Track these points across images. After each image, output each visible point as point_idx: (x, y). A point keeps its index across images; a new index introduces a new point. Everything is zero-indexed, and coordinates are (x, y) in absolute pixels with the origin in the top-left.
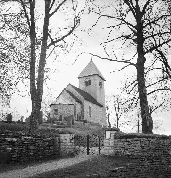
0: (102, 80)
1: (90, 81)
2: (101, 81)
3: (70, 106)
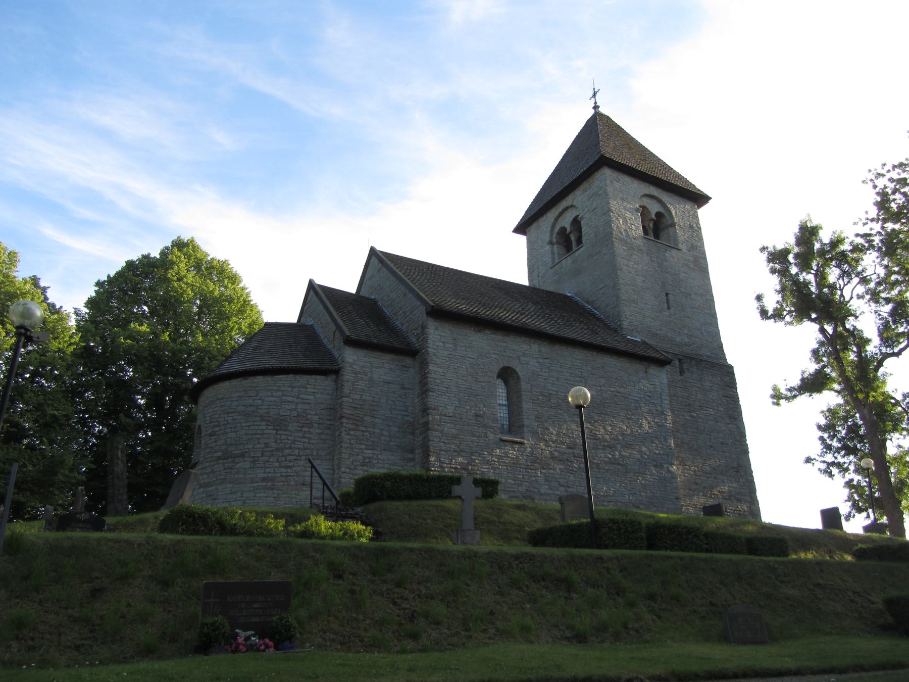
0: (666, 197)
1: (576, 222)
2: (660, 201)
3: (284, 380)
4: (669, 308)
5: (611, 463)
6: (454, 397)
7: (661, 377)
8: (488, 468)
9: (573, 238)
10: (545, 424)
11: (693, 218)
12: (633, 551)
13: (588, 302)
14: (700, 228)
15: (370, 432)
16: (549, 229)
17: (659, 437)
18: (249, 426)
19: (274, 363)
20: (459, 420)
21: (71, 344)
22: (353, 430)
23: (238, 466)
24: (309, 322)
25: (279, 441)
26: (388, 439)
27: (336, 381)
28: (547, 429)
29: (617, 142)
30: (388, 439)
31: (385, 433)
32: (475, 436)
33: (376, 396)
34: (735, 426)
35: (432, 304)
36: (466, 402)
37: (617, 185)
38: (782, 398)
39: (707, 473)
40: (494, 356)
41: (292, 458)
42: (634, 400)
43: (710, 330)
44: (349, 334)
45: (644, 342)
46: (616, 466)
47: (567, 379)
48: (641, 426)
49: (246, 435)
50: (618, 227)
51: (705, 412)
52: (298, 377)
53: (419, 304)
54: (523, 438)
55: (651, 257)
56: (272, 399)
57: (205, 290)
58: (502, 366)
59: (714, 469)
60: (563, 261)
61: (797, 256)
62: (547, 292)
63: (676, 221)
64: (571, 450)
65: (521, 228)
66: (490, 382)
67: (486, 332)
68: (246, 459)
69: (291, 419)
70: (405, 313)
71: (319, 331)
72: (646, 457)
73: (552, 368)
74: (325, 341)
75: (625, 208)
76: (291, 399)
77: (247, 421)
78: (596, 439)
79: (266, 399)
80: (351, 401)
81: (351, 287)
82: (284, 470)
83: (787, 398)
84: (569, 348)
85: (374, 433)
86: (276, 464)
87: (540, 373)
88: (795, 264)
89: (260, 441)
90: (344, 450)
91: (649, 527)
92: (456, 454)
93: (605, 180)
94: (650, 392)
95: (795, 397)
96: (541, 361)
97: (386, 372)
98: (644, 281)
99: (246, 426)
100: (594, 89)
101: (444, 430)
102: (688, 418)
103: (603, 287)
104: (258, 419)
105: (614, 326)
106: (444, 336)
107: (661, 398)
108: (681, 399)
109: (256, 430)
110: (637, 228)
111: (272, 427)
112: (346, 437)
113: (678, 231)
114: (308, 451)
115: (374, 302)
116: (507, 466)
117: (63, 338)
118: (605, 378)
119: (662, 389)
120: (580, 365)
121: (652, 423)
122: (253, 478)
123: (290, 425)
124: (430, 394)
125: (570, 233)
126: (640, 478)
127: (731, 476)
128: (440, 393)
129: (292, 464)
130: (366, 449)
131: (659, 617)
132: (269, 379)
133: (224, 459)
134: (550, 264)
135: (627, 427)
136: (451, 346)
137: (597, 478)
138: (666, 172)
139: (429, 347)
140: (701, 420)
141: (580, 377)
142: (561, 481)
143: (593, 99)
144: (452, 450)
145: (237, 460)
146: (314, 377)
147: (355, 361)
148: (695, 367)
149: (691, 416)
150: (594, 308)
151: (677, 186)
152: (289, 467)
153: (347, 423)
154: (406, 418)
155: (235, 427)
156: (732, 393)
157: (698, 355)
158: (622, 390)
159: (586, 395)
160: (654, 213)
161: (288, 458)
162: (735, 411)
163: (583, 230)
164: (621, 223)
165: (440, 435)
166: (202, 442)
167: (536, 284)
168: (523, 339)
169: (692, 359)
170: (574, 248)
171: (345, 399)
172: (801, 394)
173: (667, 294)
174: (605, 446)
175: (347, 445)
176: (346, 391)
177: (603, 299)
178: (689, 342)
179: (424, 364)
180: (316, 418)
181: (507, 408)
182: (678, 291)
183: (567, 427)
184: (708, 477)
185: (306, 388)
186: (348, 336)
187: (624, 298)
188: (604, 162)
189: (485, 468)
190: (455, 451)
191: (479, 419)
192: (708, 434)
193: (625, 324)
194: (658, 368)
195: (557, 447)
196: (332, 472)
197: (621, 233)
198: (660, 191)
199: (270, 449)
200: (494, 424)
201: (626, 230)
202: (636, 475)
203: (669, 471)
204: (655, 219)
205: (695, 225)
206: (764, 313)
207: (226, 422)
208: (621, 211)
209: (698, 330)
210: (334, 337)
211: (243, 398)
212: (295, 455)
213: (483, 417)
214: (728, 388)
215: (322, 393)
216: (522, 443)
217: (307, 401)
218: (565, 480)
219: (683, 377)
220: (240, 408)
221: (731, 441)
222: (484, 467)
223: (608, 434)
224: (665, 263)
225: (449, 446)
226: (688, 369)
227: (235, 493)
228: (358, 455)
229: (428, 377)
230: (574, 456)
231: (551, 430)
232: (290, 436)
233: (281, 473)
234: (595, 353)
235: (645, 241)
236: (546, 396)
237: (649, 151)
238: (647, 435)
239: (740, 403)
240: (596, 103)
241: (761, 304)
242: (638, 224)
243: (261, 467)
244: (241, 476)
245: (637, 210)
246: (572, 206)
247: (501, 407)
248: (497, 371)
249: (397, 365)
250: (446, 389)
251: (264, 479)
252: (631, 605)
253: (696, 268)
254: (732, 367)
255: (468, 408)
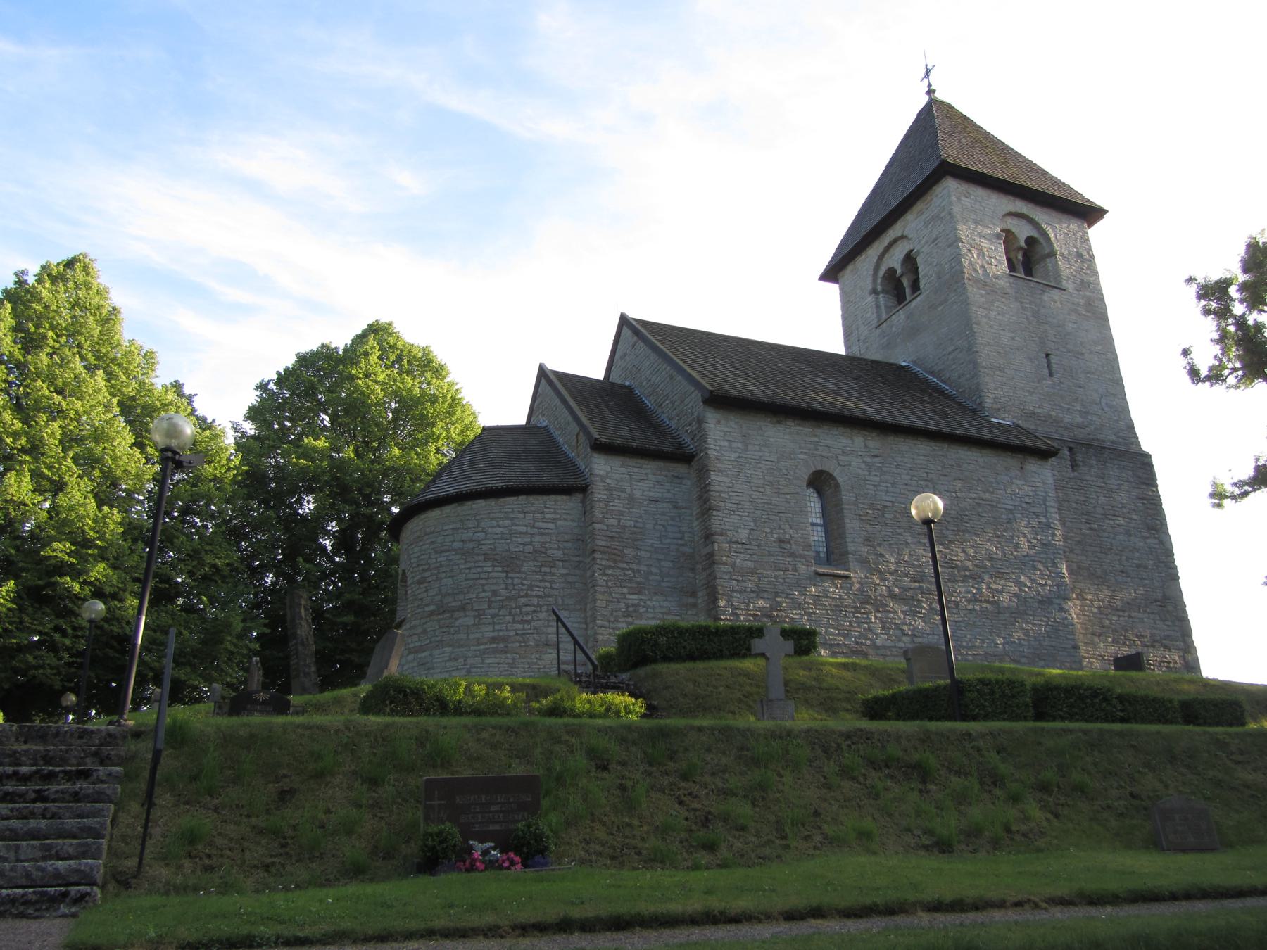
0: (1039, 215)
1: (910, 260)
3: (512, 504)
4: (1051, 375)
5: (977, 600)
6: (748, 516)
7: (1044, 475)
8: (800, 614)
9: (906, 282)
10: (878, 548)
11: (1082, 243)
12: (1014, 724)
13: (932, 373)
14: (1092, 256)
15: (633, 570)
16: (871, 272)
17: (1044, 561)
18: (469, 568)
19: (497, 482)
20: (756, 548)
21: (229, 469)
22: (610, 567)
23: (457, 623)
24: (543, 422)
25: (511, 588)
26: (658, 578)
27: (583, 502)
28: (882, 555)
29: (963, 141)
30: (658, 578)
31: (654, 570)
32: (780, 570)
33: (640, 520)
34: (1156, 541)
35: (710, 388)
36: (765, 522)
37: (966, 202)
38: (1227, 497)
39: (1118, 610)
40: (802, 456)
41: (528, 609)
42: (1006, 509)
43: (1114, 403)
44: (598, 437)
45: (1017, 426)
46: (985, 605)
47: (906, 485)
48: (1017, 546)
49: (466, 580)
50: (971, 263)
51: (1111, 522)
52: (531, 498)
53: (693, 389)
54: (848, 570)
55: (1022, 303)
56: (498, 530)
57: (400, 388)
58: (814, 470)
59: (1128, 603)
60: (893, 317)
61: (1243, 287)
62: (873, 362)
63: (1056, 247)
64: (917, 584)
65: (832, 274)
66: (797, 493)
67: (788, 423)
68: (467, 613)
69: (525, 557)
70: (673, 403)
71: (557, 434)
72: (1027, 590)
73: (885, 469)
74: (566, 448)
75: (980, 235)
76: (523, 529)
77: (466, 562)
78: (953, 568)
79: (490, 530)
80: (605, 528)
81: (596, 371)
82: (520, 626)
83: (1233, 497)
84: (907, 440)
85: (639, 571)
86: (509, 618)
87: (868, 478)
88: (1241, 301)
89: (486, 588)
90: (599, 597)
91: (1035, 689)
92: (753, 595)
93: (949, 196)
94: (1029, 497)
95: (1245, 494)
96: (869, 460)
97: (652, 486)
98: (1013, 338)
99: (466, 569)
100: (926, 65)
101: (735, 563)
102: (1087, 532)
103: (953, 350)
104: (482, 558)
105: (971, 404)
106: (730, 432)
107: (1045, 504)
108: (1074, 505)
109: (479, 573)
110: (1000, 262)
111: (500, 569)
112: (601, 578)
113: (1060, 263)
114: (550, 599)
115: (630, 389)
116: (827, 610)
117: (219, 462)
118: (963, 480)
119: (1046, 493)
120: (925, 462)
121: (1033, 541)
122: (478, 639)
123: (525, 564)
124: (714, 513)
125: (902, 276)
126: (1020, 620)
127: (1153, 613)
128: (727, 512)
129: (530, 617)
130: (629, 593)
131: (1057, 816)
132: (492, 502)
133: (439, 614)
134: (875, 323)
135: (997, 548)
136: (740, 445)
137: (956, 622)
138: (1039, 178)
139: (710, 449)
140: (1106, 535)
141: (926, 480)
142: (905, 628)
143: (926, 81)
144: (749, 590)
145: (456, 615)
146: (553, 497)
147: (608, 473)
148: (1093, 458)
149: (1090, 529)
150: (942, 381)
151: (1055, 197)
152: (528, 622)
153: (601, 559)
154: (682, 549)
155: (451, 571)
156: (1150, 493)
157: (1098, 440)
158: (987, 496)
159: (935, 503)
160: (1025, 237)
161: (524, 609)
162: (1157, 519)
163: (920, 270)
164: (975, 256)
165: (731, 569)
166: (409, 592)
167: (856, 352)
168: (842, 430)
169: (1090, 446)
170: (908, 298)
171: (597, 526)
172: (1255, 490)
173: (1047, 355)
174: (966, 576)
175: (603, 589)
176: (598, 514)
177: (954, 367)
178: (1083, 422)
179: (703, 472)
180: (558, 554)
181: (823, 528)
182: (1064, 350)
183: (910, 552)
184: (1119, 616)
185: (543, 513)
186: (596, 439)
187: (984, 363)
188: (947, 170)
189: (796, 614)
190: (752, 592)
191: (783, 545)
192: (1117, 554)
193: (988, 401)
194: (1039, 463)
195: (897, 580)
196: (584, 626)
197: (976, 271)
198: (1030, 205)
199: (498, 598)
200: (806, 553)
201: (982, 267)
202: (1013, 615)
203: (1062, 610)
204: (1026, 247)
205: (1084, 253)
206: (1194, 373)
207: (438, 564)
208: (974, 240)
209: (1096, 404)
210: (577, 442)
211: (460, 531)
212: (534, 606)
213: (789, 543)
214: (1144, 487)
215: (565, 520)
216: (847, 577)
217: (546, 531)
218: (911, 627)
219: (1076, 474)
220: (456, 545)
221: (1151, 562)
222: (794, 612)
223: (969, 560)
224: (1042, 311)
225: (744, 584)
226: (1083, 462)
227: (455, 659)
228: (619, 602)
229: (709, 491)
230: (922, 593)
231: (887, 556)
232: (525, 579)
233: (516, 630)
234: (946, 445)
235: (1011, 281)
236: (878, 509)
237: (1012, 149)
238: (1027, 558)
239: (1163, 507)
240: (930, 85)
241: (1190, 361)
242: (1000, 256)
243: (489, 624)
244: (463, 636)
245: (998, 236)
246: (902, 237)
247: (815, 528)
248: (807, 478)
249: (666, 476)
250: (735, 506)
251: (493, 640)
252: (1015, 799)
253: (1089, 314)
254: (1150, 456)
255: (768, 530)
